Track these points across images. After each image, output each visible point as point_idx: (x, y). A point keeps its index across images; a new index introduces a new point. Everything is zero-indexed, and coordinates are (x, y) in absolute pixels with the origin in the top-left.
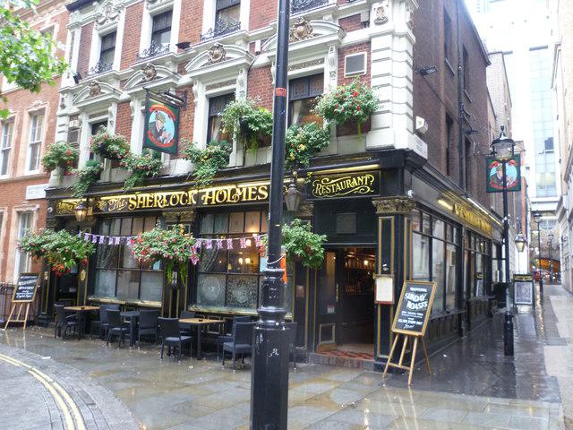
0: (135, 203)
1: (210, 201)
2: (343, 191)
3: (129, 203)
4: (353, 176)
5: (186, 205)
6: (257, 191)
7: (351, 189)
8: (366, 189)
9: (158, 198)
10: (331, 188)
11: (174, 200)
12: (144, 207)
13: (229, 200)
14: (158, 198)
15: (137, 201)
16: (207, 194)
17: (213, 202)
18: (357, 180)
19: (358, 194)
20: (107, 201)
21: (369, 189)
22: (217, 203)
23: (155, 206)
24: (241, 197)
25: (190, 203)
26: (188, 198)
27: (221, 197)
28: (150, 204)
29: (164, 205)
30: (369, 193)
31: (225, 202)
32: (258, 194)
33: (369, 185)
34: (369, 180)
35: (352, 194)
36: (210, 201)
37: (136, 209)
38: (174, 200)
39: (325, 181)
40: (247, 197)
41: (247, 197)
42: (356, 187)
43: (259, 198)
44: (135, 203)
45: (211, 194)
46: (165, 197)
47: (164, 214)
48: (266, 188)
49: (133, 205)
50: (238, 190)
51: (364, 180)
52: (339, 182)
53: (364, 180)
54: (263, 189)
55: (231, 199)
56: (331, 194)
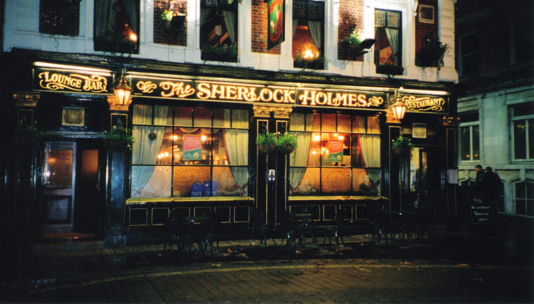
0: (208, 92)
1: (309, 102)
2: (424, 108)
3: (197, 91)
4: (431, 98)
5: (282, 103)
6: (357, 98)
7: (429, 107)
8: (440, 108)
9: (243, 90)
10: (416, 104)
11: (266, 96)
12: (222, 97)
13: (330, 103)
14: (243, 90)
15: (211, 89)
16: (306, 93)
17: (313, 103)
18: (434, 101)
19: (434, 111)
20: (157, 82)
21: (441, 109)
22: (317, 105)
23: (240, 98)
24: (342, 102)
25: (286, 101)
26: (283, 95)
27: (321, 99)
28: (232, 95)
29: (253, 99)
30: (442, 111)
31: (326, 105)
32: (357, 101)
33: (441, 105)
34: (442, 102)
35: (430, 110)
36: (309, 102)
37: (210, 98)
38: (266, 96)
39: (412, 99)
40: (348, 102)
41: (348, 102)
42: (433, 106)
43: (359, 105)
44: (208, 92)
45: (310, 95)
46: (253, 90)
47: (255, 108)
48: (364, 97)
49: (205, 95)
50: (338, 95)
51: (438, 102)
52: (421, 101)
53: (438, 102)
54: (362, 98)
55: (332, 102)
56: (416, 109)
